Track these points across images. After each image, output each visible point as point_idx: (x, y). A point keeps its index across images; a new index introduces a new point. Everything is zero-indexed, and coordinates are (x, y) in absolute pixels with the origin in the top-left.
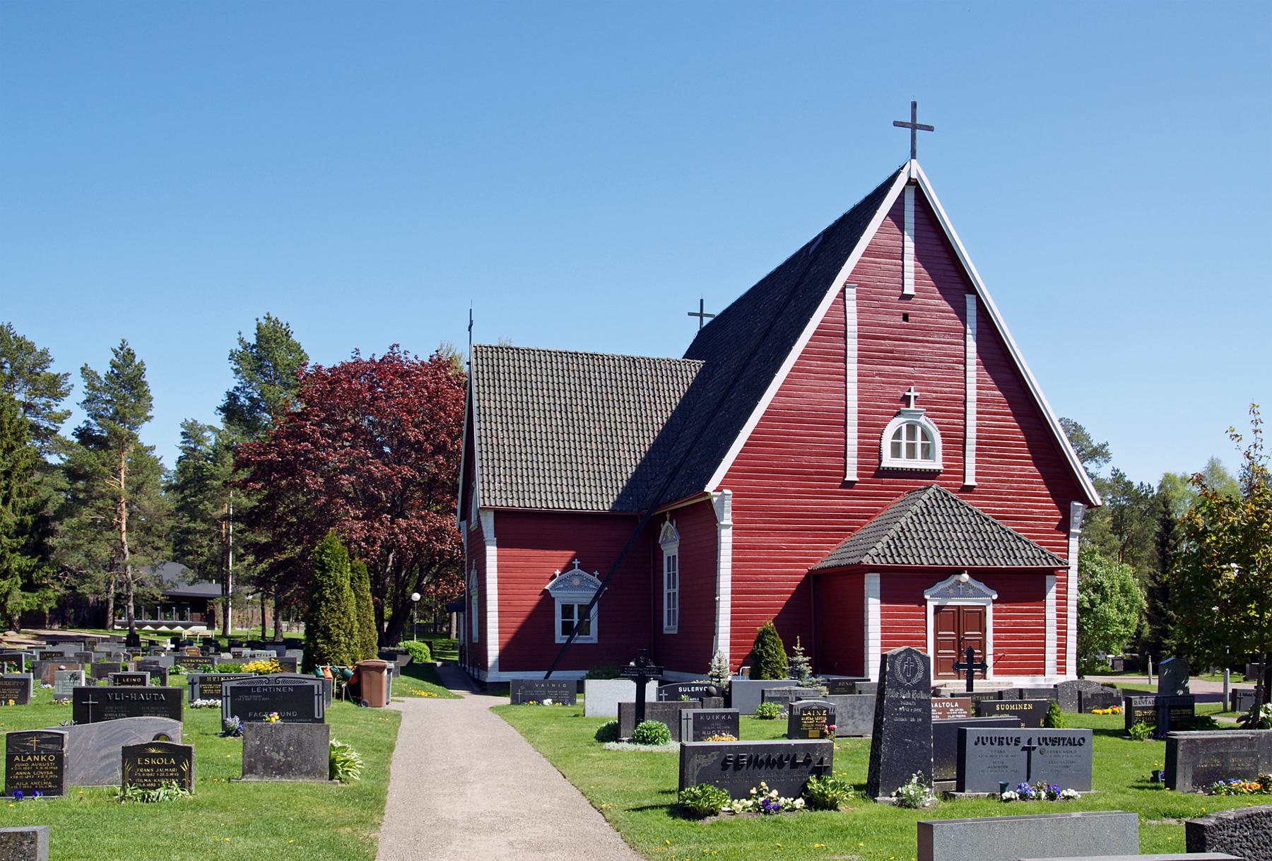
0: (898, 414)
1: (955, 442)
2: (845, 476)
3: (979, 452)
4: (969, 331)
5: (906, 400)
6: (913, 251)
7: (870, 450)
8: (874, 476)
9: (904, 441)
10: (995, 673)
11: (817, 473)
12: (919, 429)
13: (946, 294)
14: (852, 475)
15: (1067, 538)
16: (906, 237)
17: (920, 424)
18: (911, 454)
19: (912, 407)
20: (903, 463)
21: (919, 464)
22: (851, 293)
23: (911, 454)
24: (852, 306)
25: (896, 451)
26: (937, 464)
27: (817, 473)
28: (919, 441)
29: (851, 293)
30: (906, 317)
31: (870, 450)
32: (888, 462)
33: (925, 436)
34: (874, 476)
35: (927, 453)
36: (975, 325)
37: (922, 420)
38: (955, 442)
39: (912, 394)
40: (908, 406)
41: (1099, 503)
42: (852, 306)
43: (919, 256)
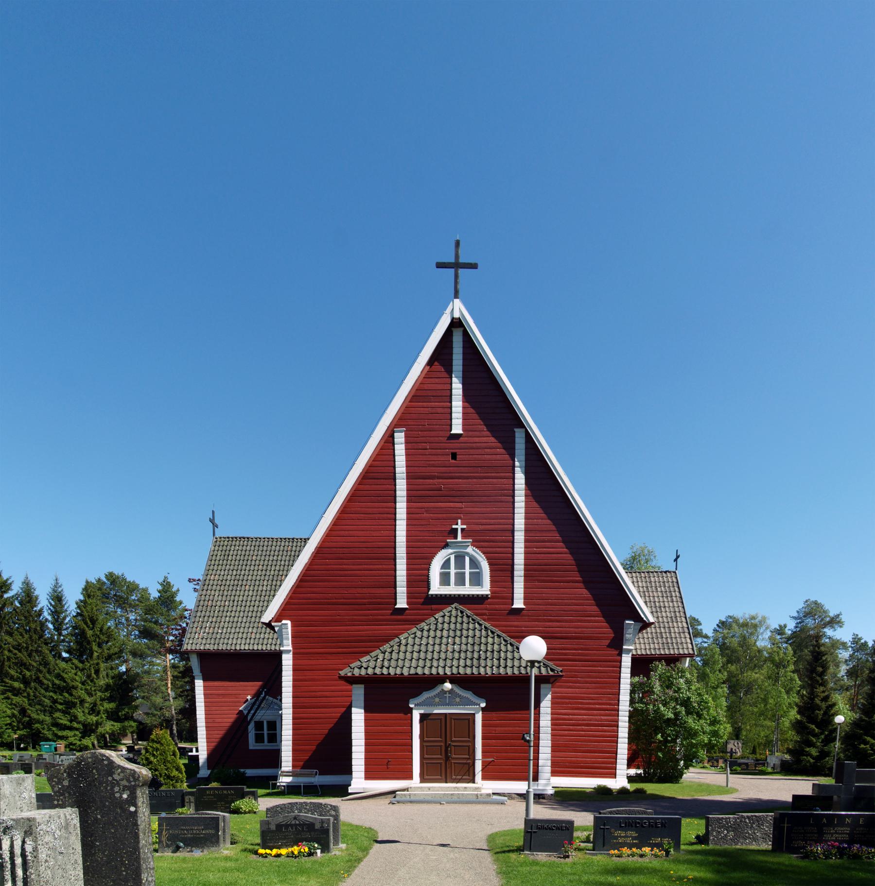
0: (446, 546)
1: (502, 570)
2: (396, 604)
3: (527, 577)
4: (517, 464)
5: (454, 533)
6: (460, 392)
7: (419, 579)
8: (423, 604)
9: (453, 571)
10: (485, 778)
11: (370, 604)
12: (467, 559)
13: (493, 430)
14: (402, 603)
15: (620, 655)
16: (454, 380)
17: (468, 554)
18: (460, 580)
19: (459, 539)
20: (452, 590)
21: (467, 590)
22: (400, 438)
23: (460, 580)
24: (400, 450)
25: (445, 579)
26: (485, 589)
27: (370, 604)
28: (467, 570)
29: (400, 438)
30: (454, 456)
31: (419, 579)
32: (436, 588)
33: (474, 563)
34: (423, 604)
35: (476, 580)
36: (523, 458)
37: (470, 550)
38: (502, 570)
39: (459, 526)
40: (456, 538)
41: (652, 620)
42: (400, 450)
43: (467, 396)
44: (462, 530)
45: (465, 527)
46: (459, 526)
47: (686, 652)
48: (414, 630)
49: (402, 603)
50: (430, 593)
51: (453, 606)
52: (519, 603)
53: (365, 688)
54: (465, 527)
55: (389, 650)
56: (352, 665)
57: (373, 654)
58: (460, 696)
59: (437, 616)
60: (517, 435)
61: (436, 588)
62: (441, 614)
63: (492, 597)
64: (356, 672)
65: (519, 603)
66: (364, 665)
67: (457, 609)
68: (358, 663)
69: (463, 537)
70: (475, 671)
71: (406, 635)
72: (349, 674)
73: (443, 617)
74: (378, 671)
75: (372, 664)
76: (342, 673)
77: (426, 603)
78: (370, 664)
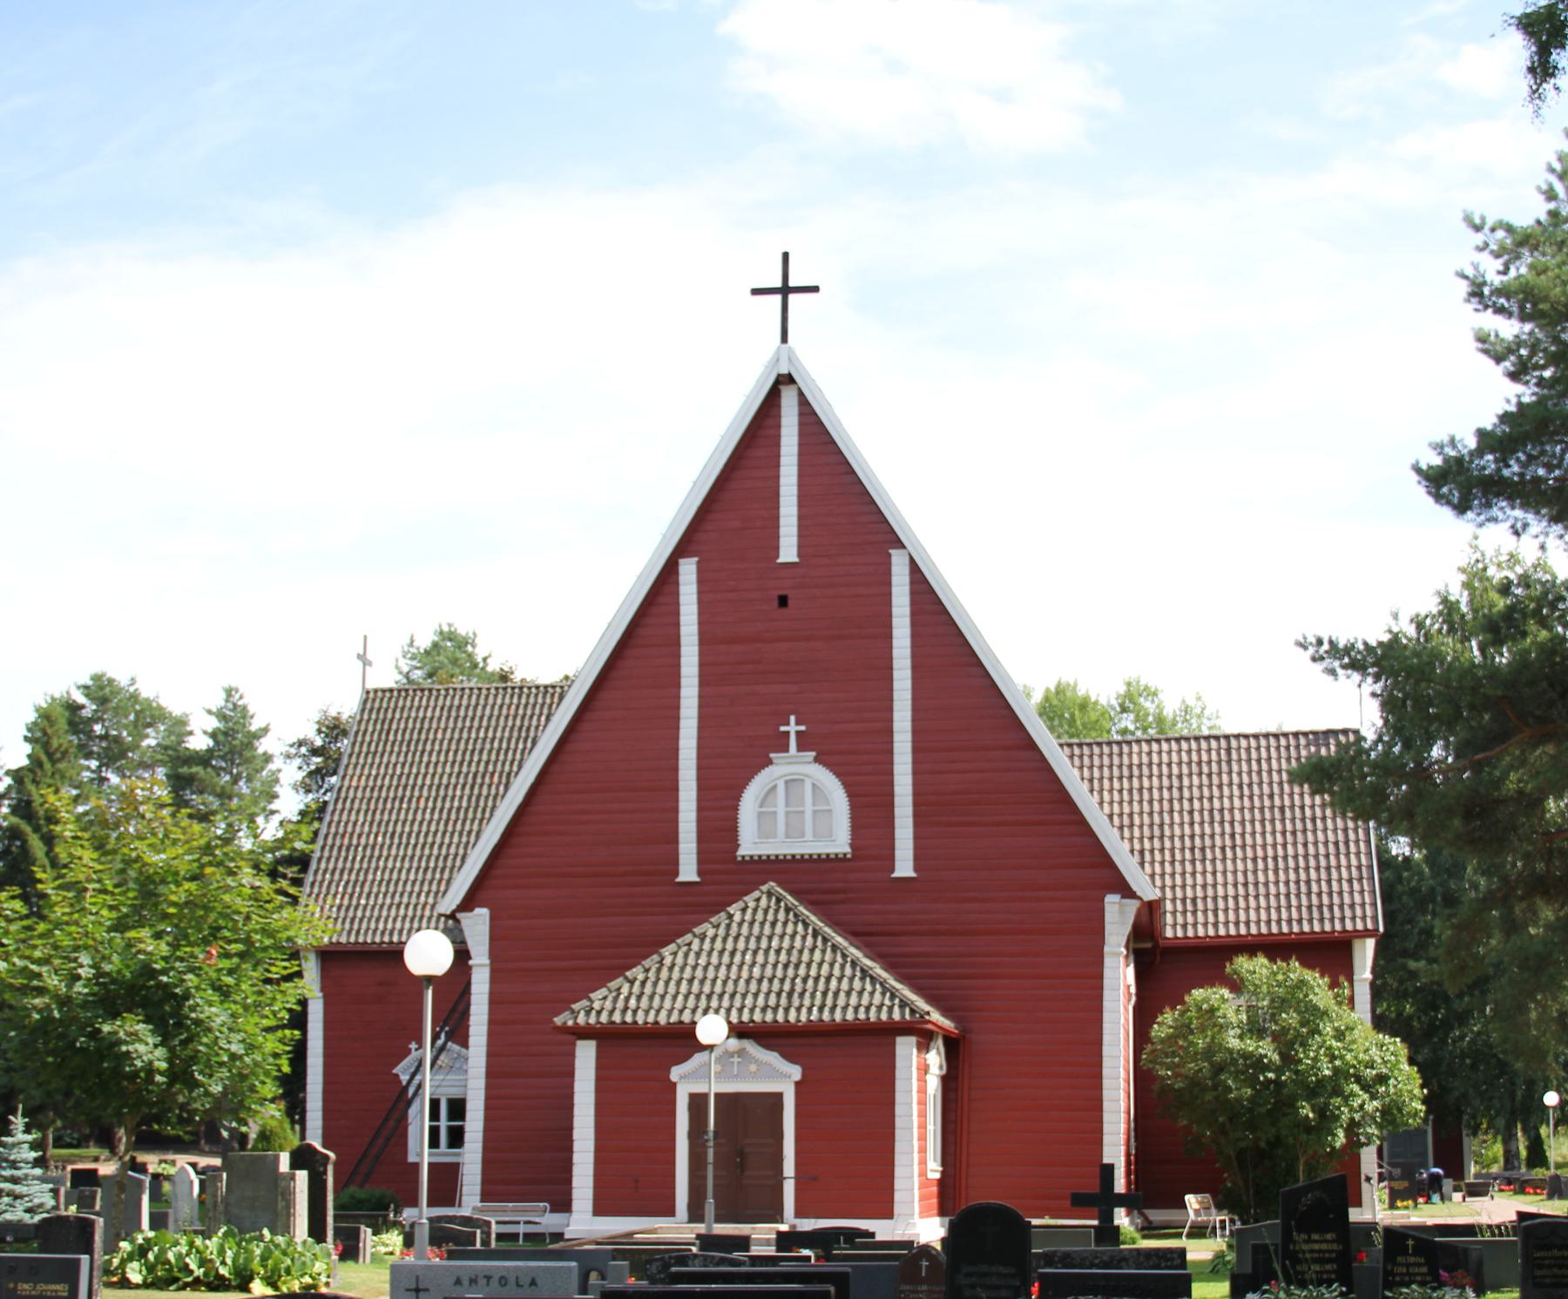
1: (870, 809)
14: (688, 871)
31: (719, 827)
32: (751, 843)
44: (798, 733)
45: (803, 728)
46: (792, 728)
47: (1360, 926)
48: (688, 937)
49: (688, 871)
50: (741, 852)
51: (764, 888)
52: (904, 867)
53: (598, 1047)
54: (803, 728)
55: (641, 977)
56: (576, 1006)
57: (613, 985)
58: (756, 1061)
59: (731, 910)
60: (894, 560)
61: (751, 843)
62: (740, 904)
63: (855, 857)
64: (581, 1020)
65: (904, 867)
66: (597, 1005)
67: (770, 894)
68: (585, 1003)
69: (801, 748)
70: (780, 1017)
71: (672, 947)
72: (570, 1023)
73: (744, 910)
74: (617, 1018)
75: (608, 1004)
76: (558, 1020)
77: (730, 876)
78: (607, 1004)
